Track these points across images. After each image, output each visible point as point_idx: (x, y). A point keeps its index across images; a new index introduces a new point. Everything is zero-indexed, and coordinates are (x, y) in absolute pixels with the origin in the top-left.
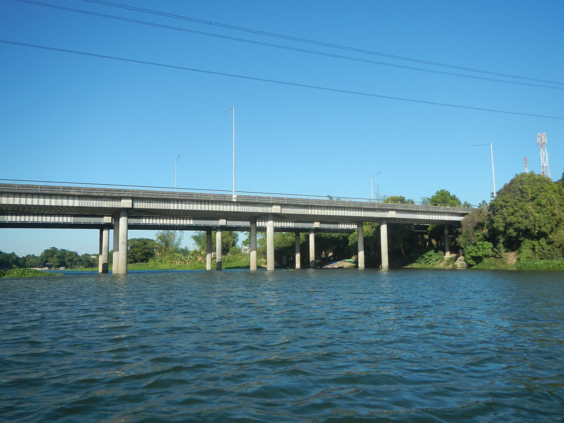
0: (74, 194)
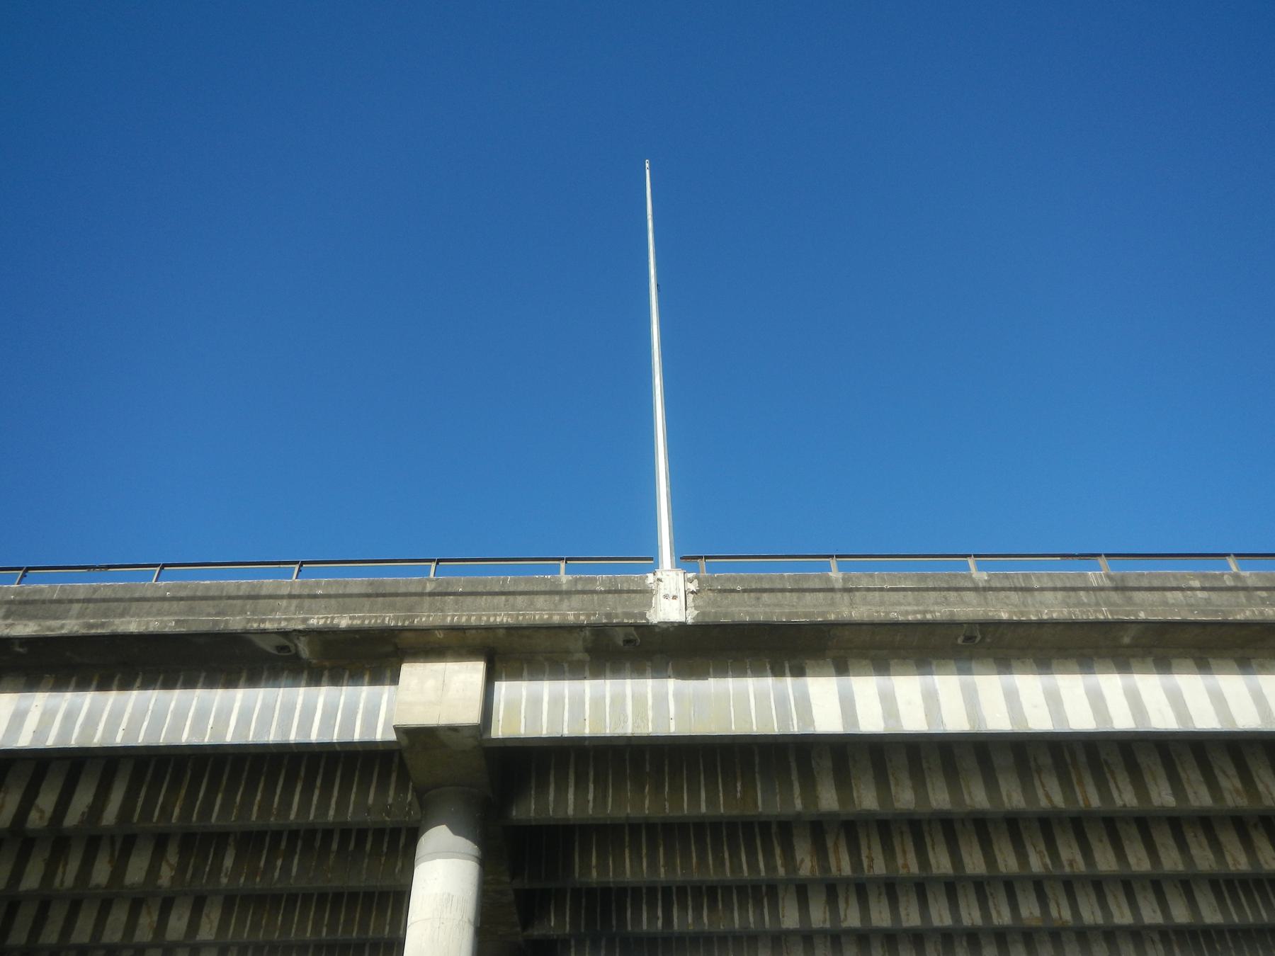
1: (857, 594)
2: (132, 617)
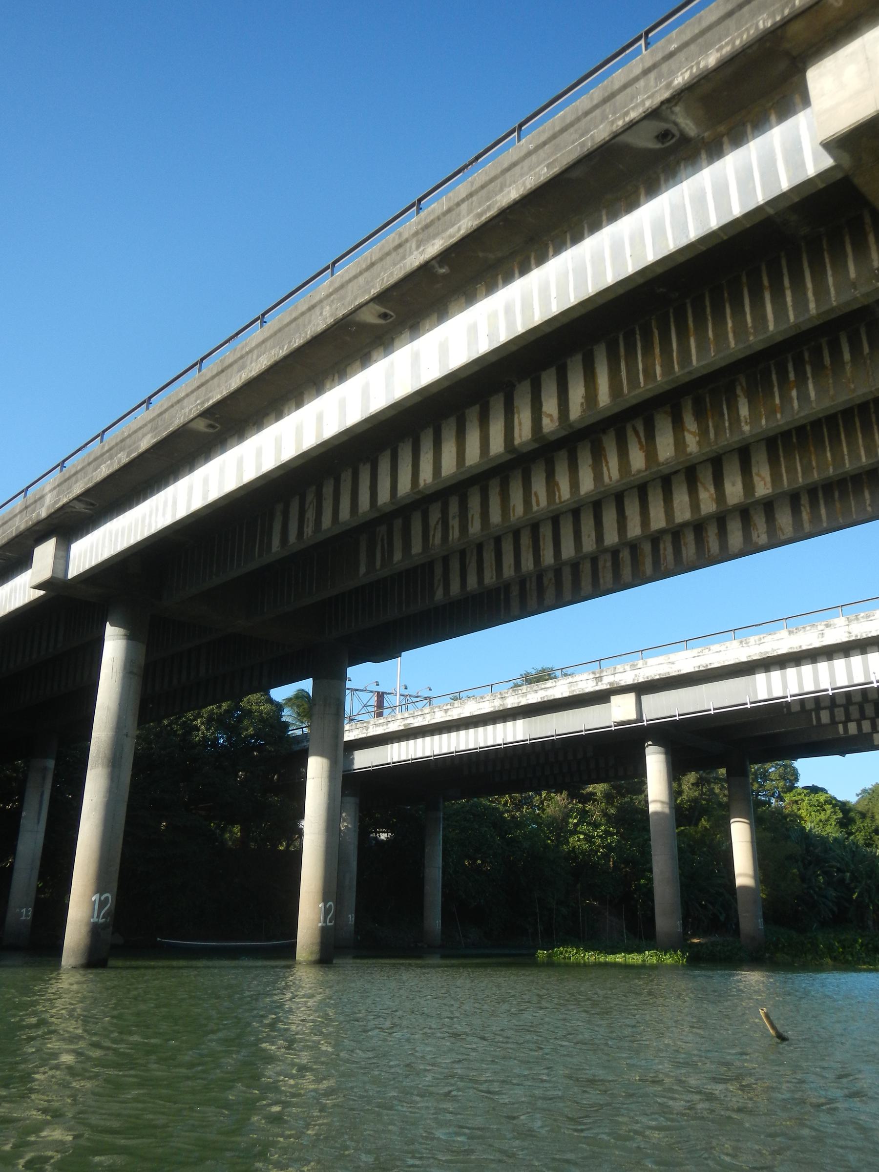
2: (510, 186)
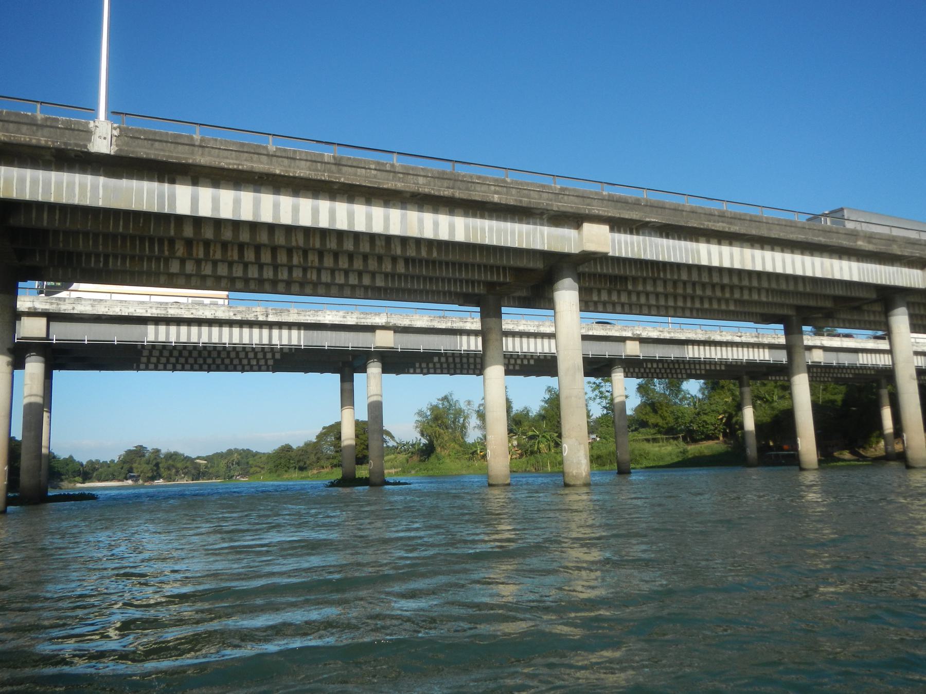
0: (863, 248)
1: (207, 149)
